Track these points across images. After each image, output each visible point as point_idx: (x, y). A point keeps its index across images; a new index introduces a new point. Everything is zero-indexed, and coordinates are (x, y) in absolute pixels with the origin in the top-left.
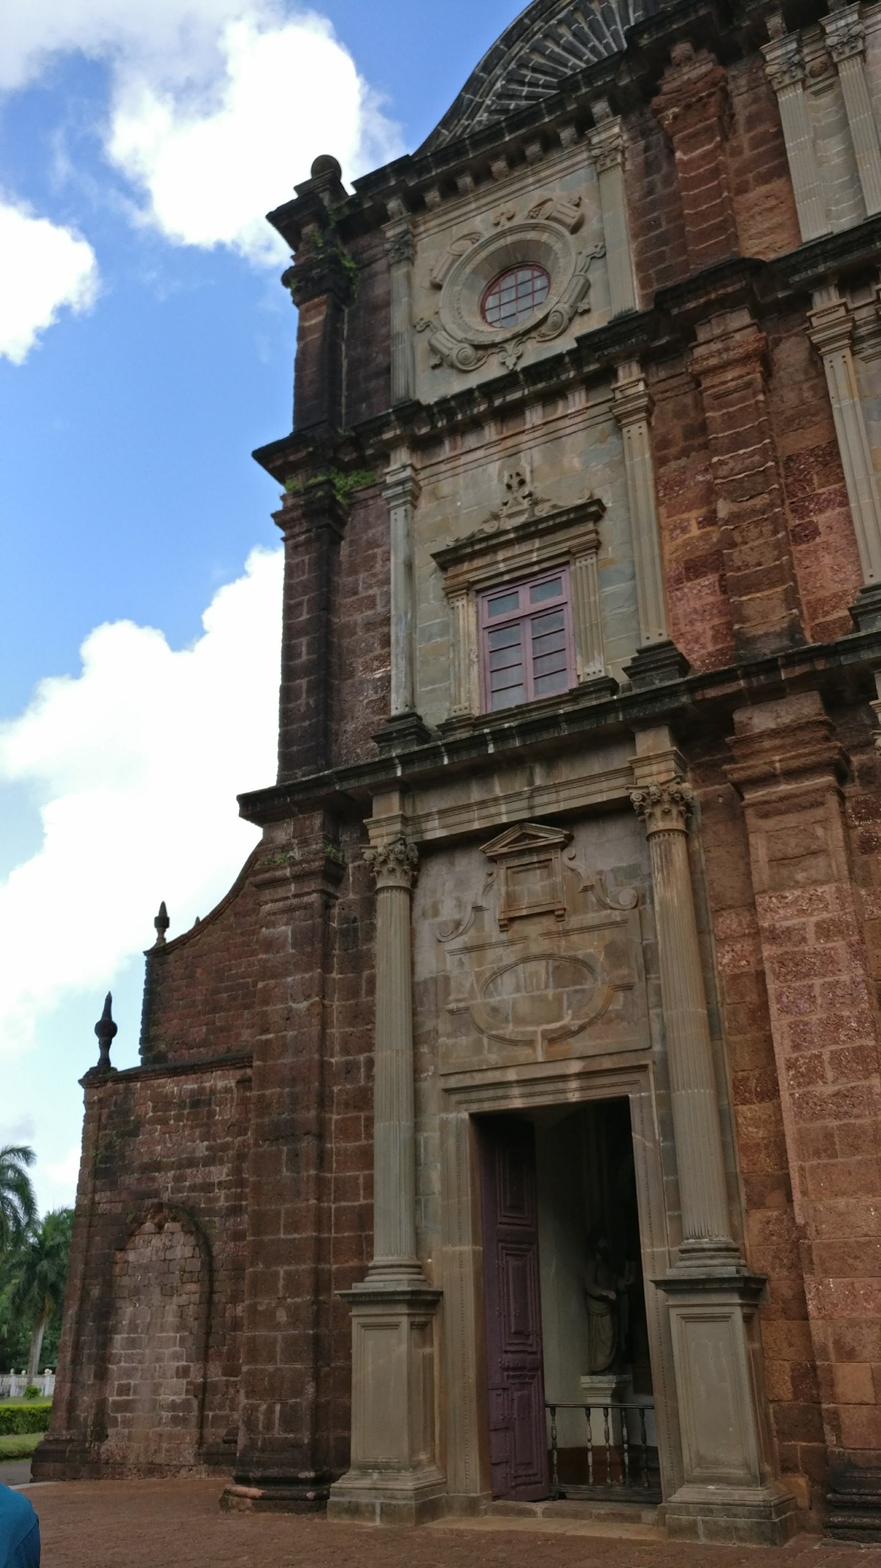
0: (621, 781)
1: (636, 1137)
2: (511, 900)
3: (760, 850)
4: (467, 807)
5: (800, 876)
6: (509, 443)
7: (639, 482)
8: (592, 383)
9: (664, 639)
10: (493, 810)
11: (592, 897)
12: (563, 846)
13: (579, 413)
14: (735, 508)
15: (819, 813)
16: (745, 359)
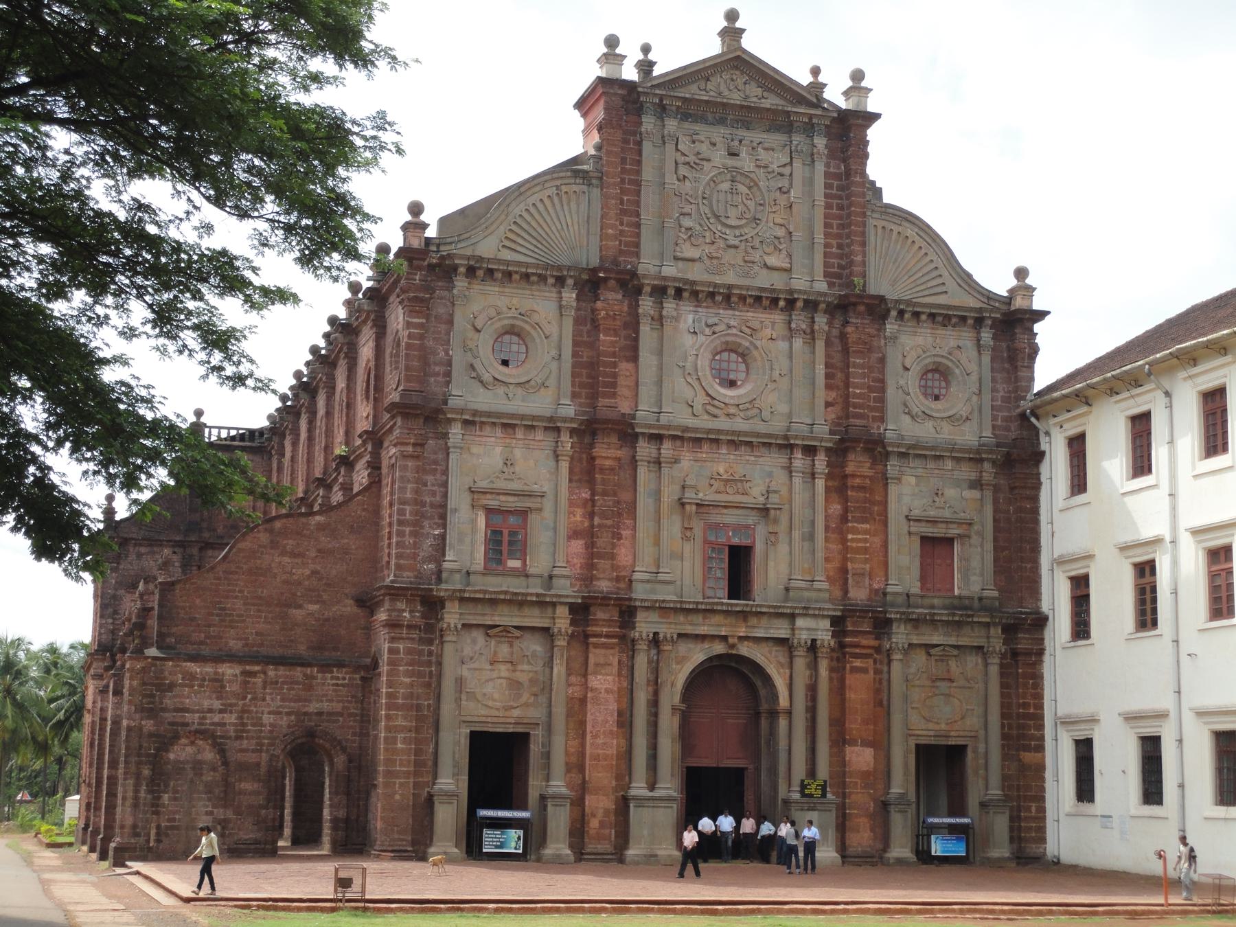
0: (548, 621)
1: (532, 746)
2: (495, 652)
3: (592, 660)
4: (485, 615)
5: (603, 671)
6: (507, 441)
7: (563, 490)
8: (546, 428)
9: (564, 565)
10: (496, 618)
11: (525, 658)
12: (518, 638)
13: (540, 441)
14: (600, 521)
15: (612, 651)
16: (615, 459)
